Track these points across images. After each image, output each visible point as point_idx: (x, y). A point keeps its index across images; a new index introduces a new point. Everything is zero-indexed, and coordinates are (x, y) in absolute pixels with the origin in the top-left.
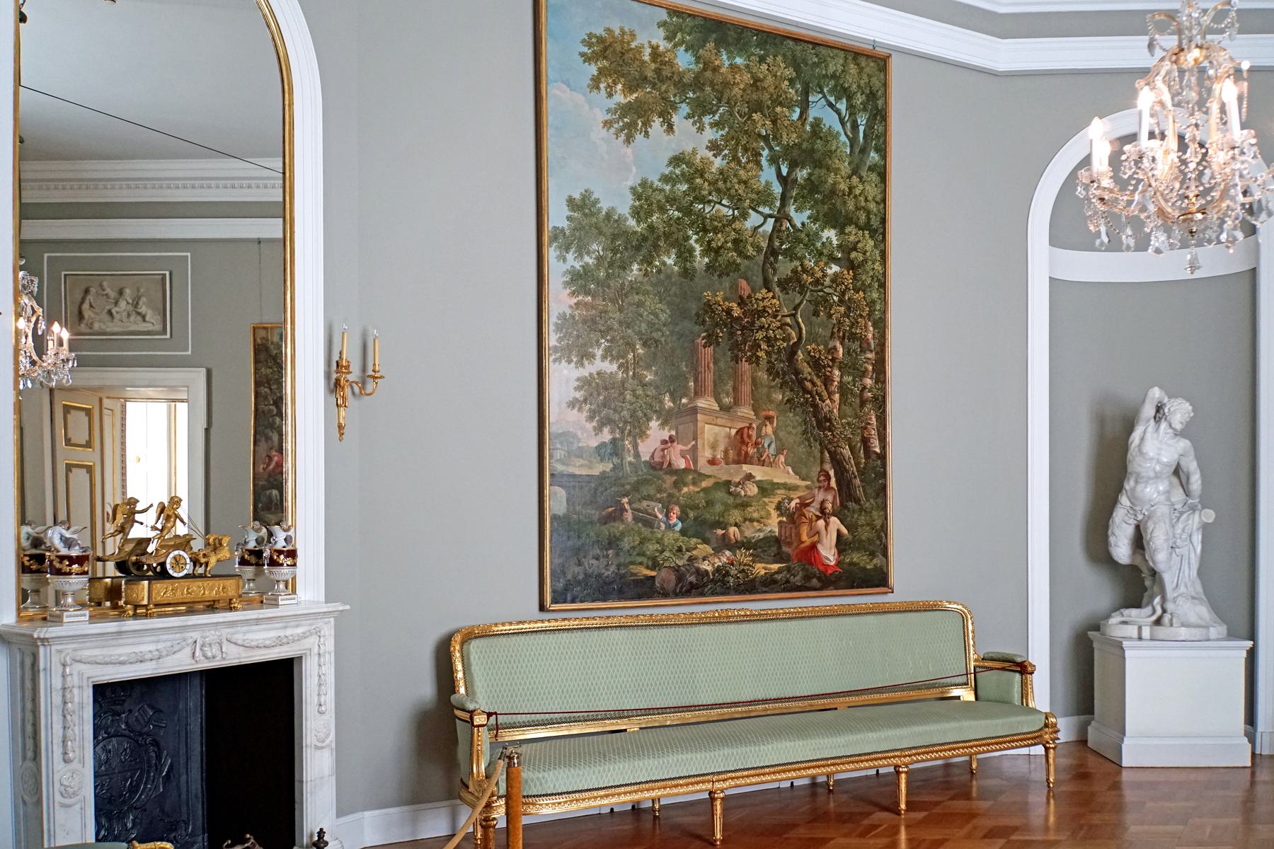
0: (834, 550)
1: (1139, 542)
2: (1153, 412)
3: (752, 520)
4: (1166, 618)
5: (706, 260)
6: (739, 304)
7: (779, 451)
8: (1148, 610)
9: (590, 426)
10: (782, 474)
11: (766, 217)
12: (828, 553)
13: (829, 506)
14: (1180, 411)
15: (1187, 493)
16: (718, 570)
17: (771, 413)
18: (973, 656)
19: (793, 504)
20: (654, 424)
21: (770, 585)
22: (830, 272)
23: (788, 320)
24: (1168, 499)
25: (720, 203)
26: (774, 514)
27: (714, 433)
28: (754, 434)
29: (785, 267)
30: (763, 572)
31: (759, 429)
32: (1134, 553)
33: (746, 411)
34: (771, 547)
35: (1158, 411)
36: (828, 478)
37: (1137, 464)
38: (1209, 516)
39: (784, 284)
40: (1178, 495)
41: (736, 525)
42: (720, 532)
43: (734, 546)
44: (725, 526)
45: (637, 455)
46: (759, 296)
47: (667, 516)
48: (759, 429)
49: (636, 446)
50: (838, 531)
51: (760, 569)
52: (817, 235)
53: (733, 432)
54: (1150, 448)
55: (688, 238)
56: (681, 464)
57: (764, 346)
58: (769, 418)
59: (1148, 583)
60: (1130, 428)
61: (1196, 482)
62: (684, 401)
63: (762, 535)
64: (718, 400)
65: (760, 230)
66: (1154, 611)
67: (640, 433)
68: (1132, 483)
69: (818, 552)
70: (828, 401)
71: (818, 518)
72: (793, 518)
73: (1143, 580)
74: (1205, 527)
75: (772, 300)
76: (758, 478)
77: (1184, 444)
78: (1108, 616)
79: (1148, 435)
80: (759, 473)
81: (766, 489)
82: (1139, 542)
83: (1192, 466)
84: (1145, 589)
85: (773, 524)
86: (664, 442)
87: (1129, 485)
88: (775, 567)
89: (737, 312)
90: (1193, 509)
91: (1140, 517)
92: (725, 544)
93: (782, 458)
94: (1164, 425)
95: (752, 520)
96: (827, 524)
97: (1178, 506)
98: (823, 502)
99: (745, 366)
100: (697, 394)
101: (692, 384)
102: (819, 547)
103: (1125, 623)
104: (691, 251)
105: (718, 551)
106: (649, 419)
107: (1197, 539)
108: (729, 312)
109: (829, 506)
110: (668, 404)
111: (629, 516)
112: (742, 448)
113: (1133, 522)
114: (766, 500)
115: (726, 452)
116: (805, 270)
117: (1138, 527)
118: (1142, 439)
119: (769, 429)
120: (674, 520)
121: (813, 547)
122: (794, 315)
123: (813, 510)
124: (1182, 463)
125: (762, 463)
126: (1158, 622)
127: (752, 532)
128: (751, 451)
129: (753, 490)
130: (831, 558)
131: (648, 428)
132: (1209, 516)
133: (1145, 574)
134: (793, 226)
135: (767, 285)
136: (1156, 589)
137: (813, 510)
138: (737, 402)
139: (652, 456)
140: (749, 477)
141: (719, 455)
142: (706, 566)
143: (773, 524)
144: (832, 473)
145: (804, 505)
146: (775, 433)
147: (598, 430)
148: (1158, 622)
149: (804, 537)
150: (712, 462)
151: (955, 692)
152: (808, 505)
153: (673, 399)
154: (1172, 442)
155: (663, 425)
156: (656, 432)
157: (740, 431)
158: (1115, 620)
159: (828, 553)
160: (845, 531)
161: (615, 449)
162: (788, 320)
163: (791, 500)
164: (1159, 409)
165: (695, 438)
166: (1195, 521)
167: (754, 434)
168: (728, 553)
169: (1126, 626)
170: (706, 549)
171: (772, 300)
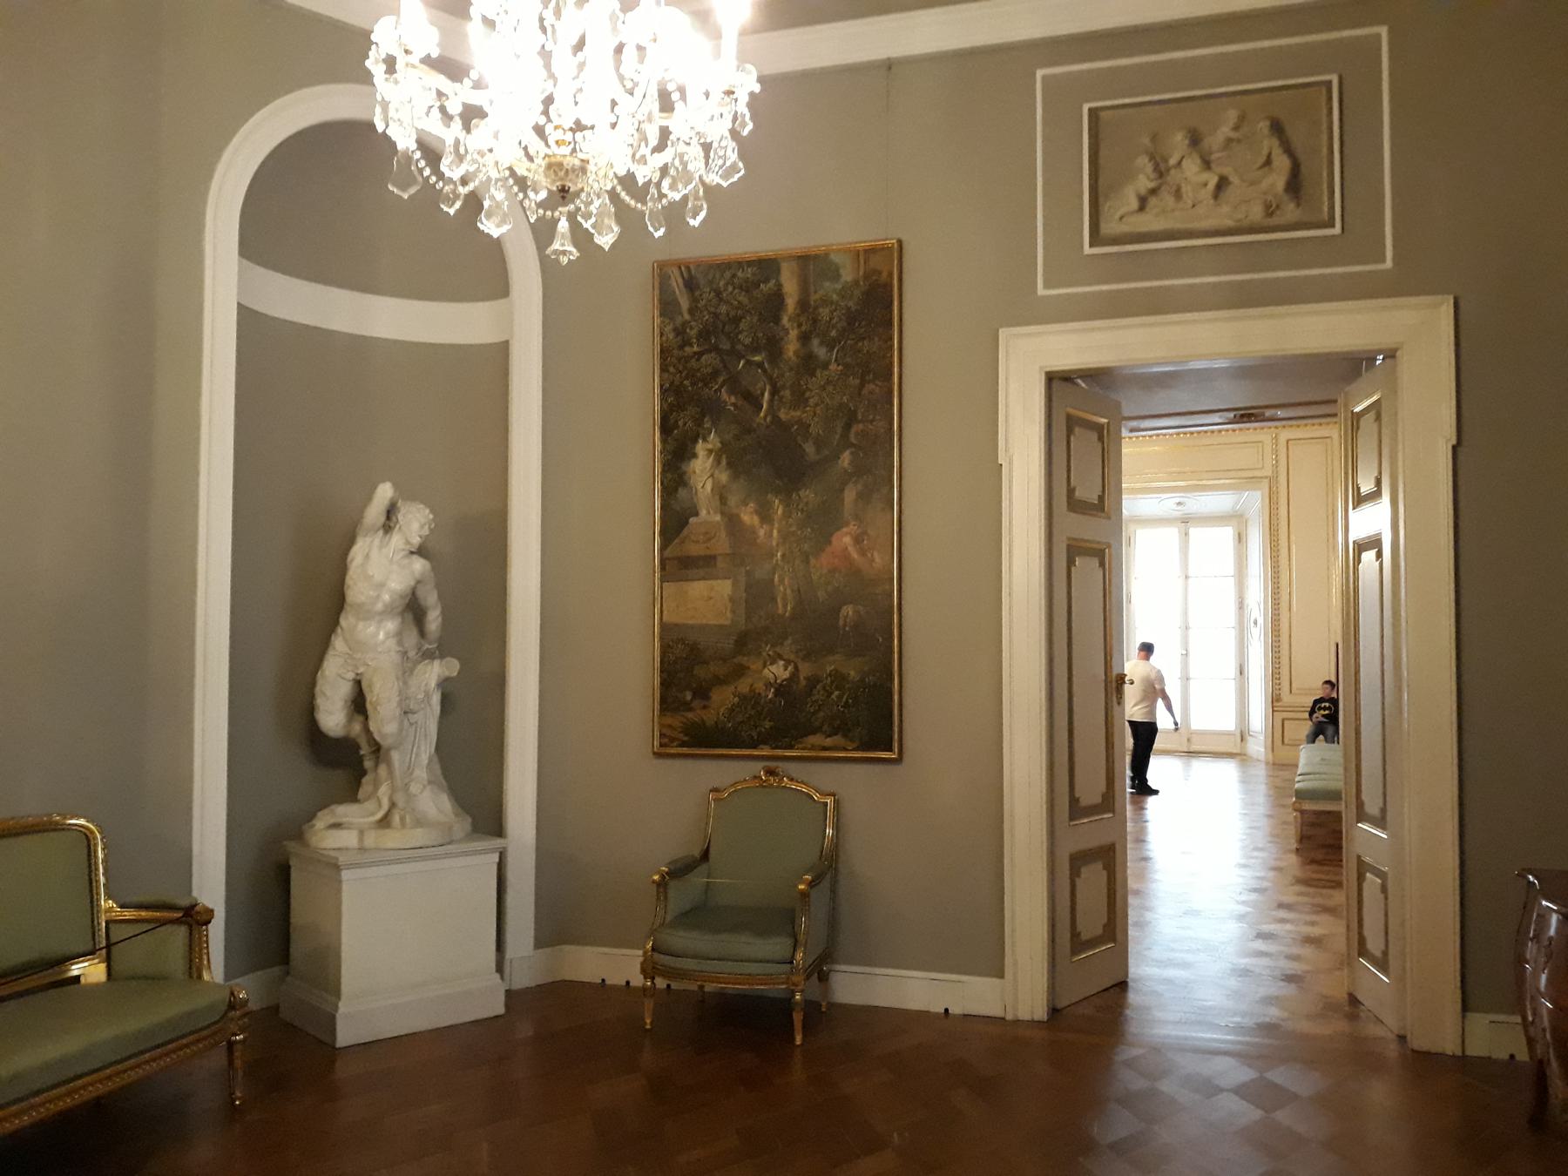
1: (359, 704)
2: (383, 519)
4: (396, 819)
8: (369, 805)
14: (416, 522)
15: (422, 633)
18: (105, 903)
24: (400, 643)
32: (350, 720)
35: (388, 518)
37: (357, 590)
38: (448, 667)
40: (412, 638)
54: (376, 569)
59: (368, 764)
60: (351, 541)
61: (434, 620)
66: (380, 805)
68: (352, 620)
73: (360, 760)
74: (446, 687)
77: (419, 565)
78: (312, 816)
79: (374, 554)
82: (359, 704)
83: (430, 599)
84: (364, 773)
87: (346, 621)
90: (428, 656)
91: (361, 670)
94: (396, 540)
97: (412, 654)
103: (337, 826)
107: (436, 699)
113: (351, 676)
117: (358, 683)
118: (367, 556)
124: (420, 593)
126: (385, 822)
132: (448, 667)
133: (365, 750)
136: (382, 770)
148: (385, 822)
151: (76, 969)
154: (406, 561)
158: (322, 820)
164: (391, 512)
166: (433, 673)
169: (340, 832)
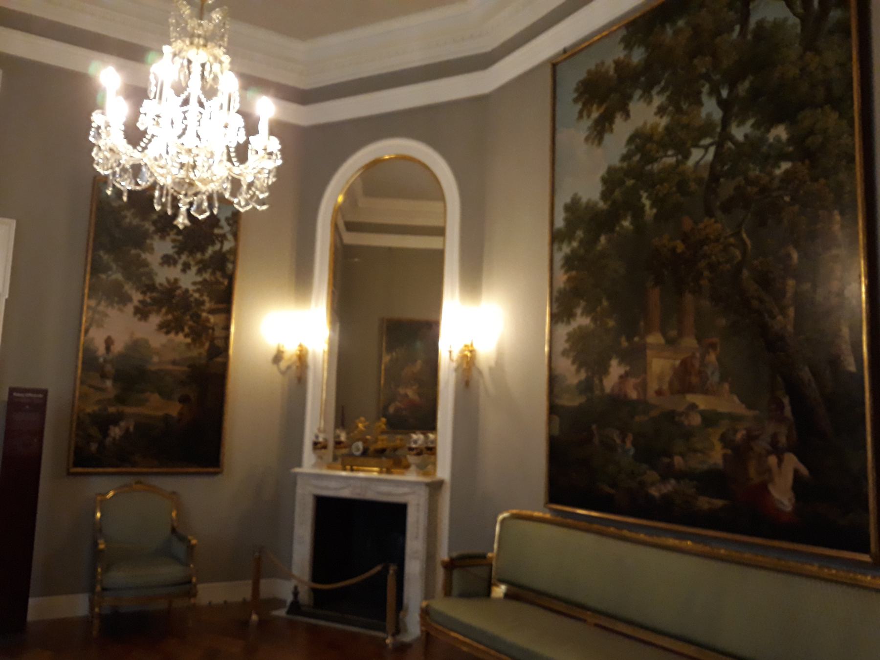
0: (791, 494)
3: (695, 451)
5: (655, 211)
6: (683, 241)
7: (723, 379)
9: (573, 368)
10: (727, 403)
11: (706, 148)
12: (782, 495)
13: (783, 440)
16: (664, 497)
17: (715, 340)
19: (739, 436)
20: (614, 362)
21: (710, 520)
22: (778, 172)
23: (732, 240)
25: (666, 156)
26: (718, 446)
27: (660, 366)
28: (697, 364)
29: (727, 188)
30: (706, 506)
31: (703, 357)
33: (690, 342)
34: (712, 481)
36: (781, 407)
39: (727, 208)
41: (682, 455)
42: (666, 460)
43: (680, 476)
44: (670, 456)
45: (602, 389)
46: (701, 226)
47: (623, 441)
48: (703, 357)
49: (601, 381)
50: (796, 472)
51: (704, 503)
52: (763, 140)
53: (678, 362)
55: (641, 197)
56: (633, 395)
57: (706, 273)
58: (713, 346)
62: (636, 339)
63: (705, 467)
64: (664, 334)
65: (702, 163)
67: (604, 370)
69: (769, 493)
70: (780, 318)
71: (769, 453)
72: (739, 453)
75: (713, 226)
76: (702, 407)
80: (702, 402)
81: (710, 419)
85: (717, 456)
86: (621, 377)
88: (719, 503)
89: (680, 247)
92: (668, 473)
93: (726, 386)
95: (695, 451)
96: (780, 461)
98: (775, 436)
99: (689, 298)
100: (648, 331)
101: (642, 323)
102: (771, 488)
104: (644, 206)
105: (664, 478)
106: (610, 358)
108: (674, 250)
109: (783, 440)
110: (625, 344)
111: (596, 440)
112: (685, 379)
114: (710, 430)
115: (671, 384)
116: (749, 182)
119: (712, 357)
120: (628, 444)
121: (763, 489)
122: (737, 234)
123: (762, 444)
125: (705, 391)
127: (697, 463)
128: (694, 380)
129: (696, 420)
130: (786, 502)
131: (610, 366)
134: (735, 143)
135: (709, 213)
137: (762, 444)
138: (681, 335)
139: (613, 389)
140: (693, 407)
141: (665, 387)
142: (654, 492)
143: (717, 456)
144: (786, 401)
145: (751, 437)
146: (718, 359)
147: (578, 371)
149: (752, 472)
150: (659, 393)
152: (756, 437)
153: (629, 339)
155: (620, 363)
156: (616, 369)
157: (684, 363)
159: (782, 495)
160: (804, 470)
161: (586, 387)
162: (732, 240)
163: (736, 431)
165: (645, 371)
167: (697, 364)
168: (673, 481)
170: (652, 476)
171: (713, 226)
